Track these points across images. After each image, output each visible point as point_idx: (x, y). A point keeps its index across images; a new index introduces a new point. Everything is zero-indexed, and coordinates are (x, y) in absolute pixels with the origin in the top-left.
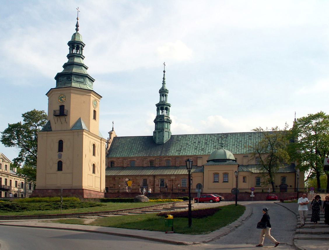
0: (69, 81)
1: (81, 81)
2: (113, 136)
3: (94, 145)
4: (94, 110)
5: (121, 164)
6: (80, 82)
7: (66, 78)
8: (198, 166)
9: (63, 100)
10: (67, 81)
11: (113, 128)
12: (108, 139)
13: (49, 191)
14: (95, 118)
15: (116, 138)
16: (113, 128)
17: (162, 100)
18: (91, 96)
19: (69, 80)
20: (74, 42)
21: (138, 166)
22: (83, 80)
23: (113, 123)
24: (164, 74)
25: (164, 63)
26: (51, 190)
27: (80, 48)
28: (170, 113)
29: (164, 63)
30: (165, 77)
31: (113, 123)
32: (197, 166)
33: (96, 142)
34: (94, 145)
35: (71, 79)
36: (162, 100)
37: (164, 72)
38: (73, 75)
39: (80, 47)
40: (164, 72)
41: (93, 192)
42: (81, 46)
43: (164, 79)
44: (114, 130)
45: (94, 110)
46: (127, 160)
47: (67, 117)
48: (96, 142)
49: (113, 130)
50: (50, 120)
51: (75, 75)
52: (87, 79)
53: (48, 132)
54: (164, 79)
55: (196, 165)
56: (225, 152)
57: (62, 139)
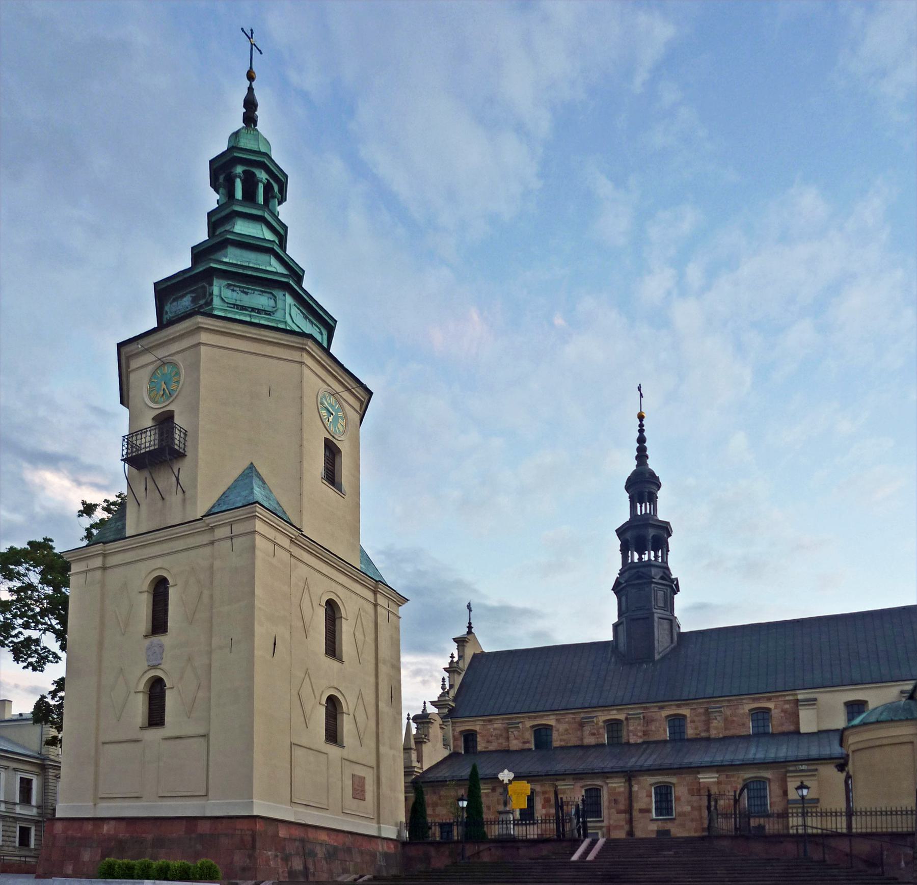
1: (260, 307)
2: (469, 652)
3: (332, 608)
4: (326, 439)
5: (500, 741)
6: (253, 310)
8: (802, 731)
11: (470, 623)
12: (452, 657)
13: (106, 828)
14: (331, 476)
15: (480, 658)
16: (470, 623)
17: (639, 513)
18: (302, 363)
21: (563, 744)
22: (272, 303)
23: (470, 611)
24: (641, 426)
25: (640, 385)
26: (112, 823)
28: (669, 556)
29: (640, 385)
30: (645, 434)
31: (470, 611)
32: (797, 732)
33: (341, 591)
34: (332, 608)
36: (639, 513)
37: (641, 417)
38: (219, 277)
40: (641, 417)
41: (323, 837)
43: (641, 440)
44: (473, 630)
45: (326, 439)
46: (520, 725)
47: (184, 467)
48: (341, 591)
49: (470, 632)
51: (229, 279)
52: (289, 299)
54: (641, 440)
55: (792, 728)
57: (165, 574)
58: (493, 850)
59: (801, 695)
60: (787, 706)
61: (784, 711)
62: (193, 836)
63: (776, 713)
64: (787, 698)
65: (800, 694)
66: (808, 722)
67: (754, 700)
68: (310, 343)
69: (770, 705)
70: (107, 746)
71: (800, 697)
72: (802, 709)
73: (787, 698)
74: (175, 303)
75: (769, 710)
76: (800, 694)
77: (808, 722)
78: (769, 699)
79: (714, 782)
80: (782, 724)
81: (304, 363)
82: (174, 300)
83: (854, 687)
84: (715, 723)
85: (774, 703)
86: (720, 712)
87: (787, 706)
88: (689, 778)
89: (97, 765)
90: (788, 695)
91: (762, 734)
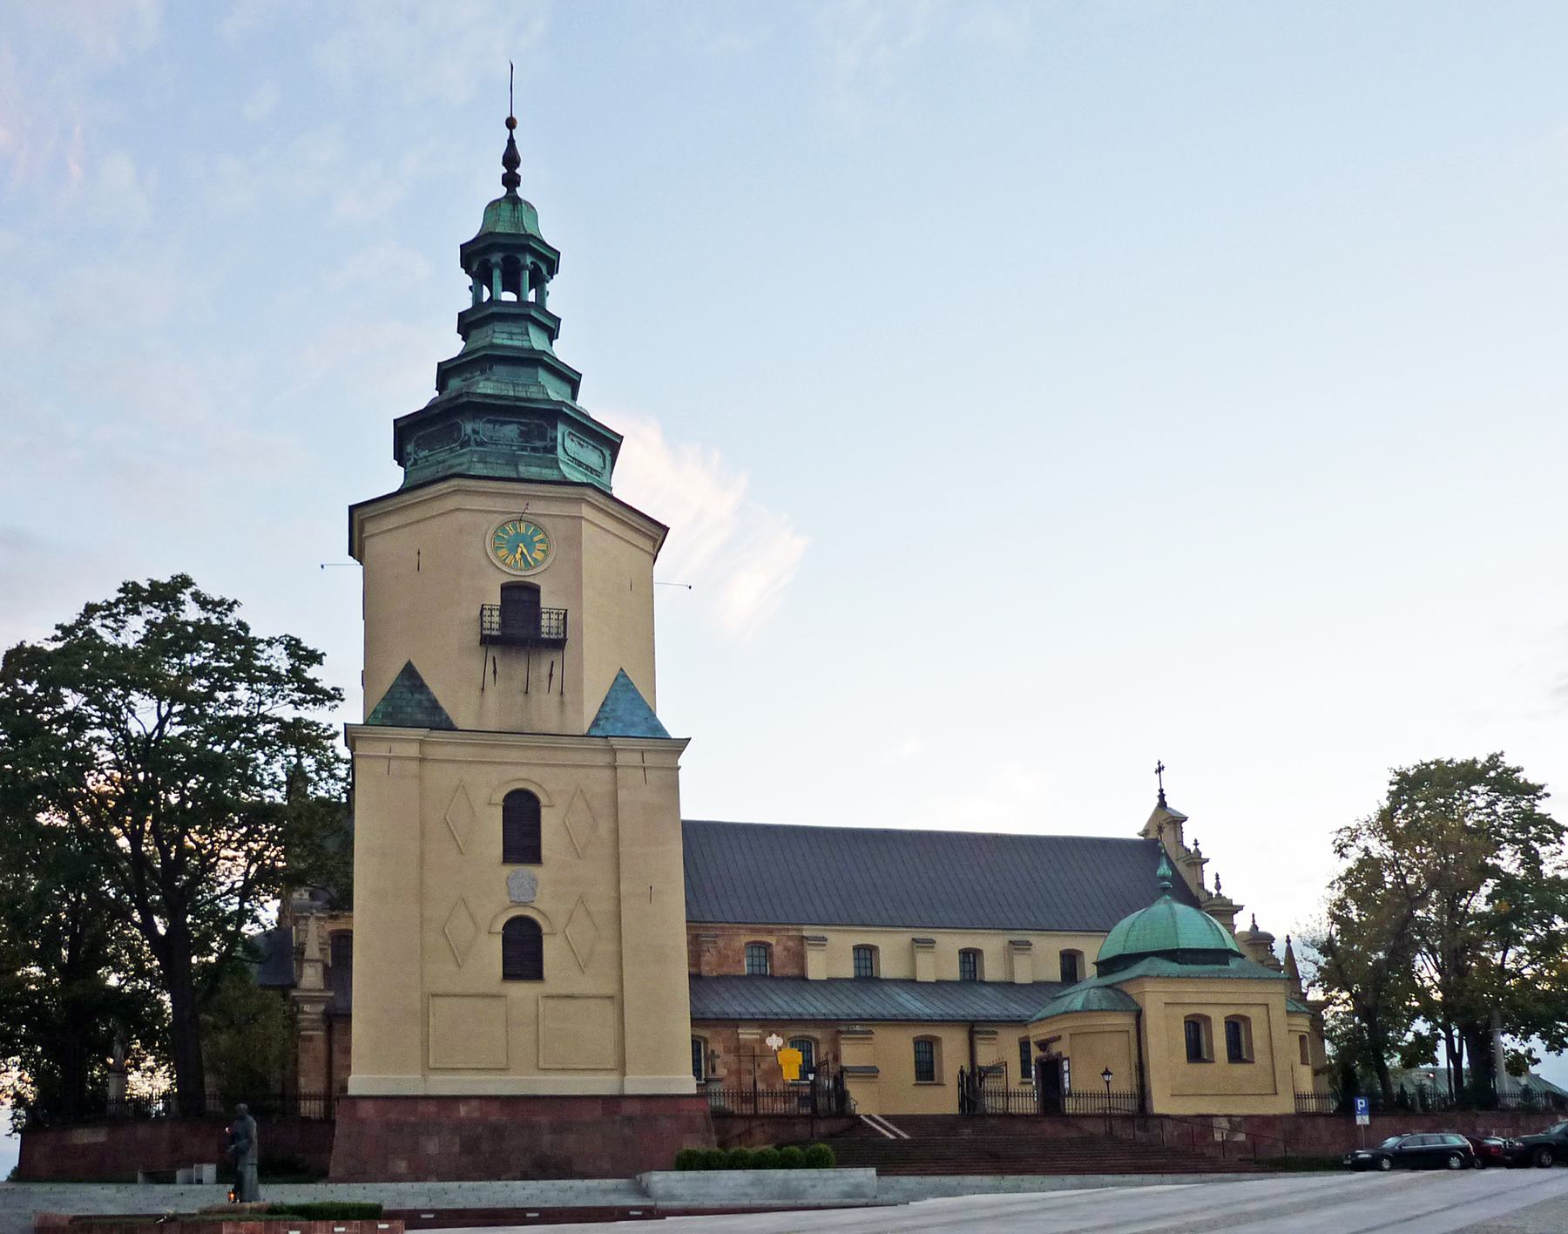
0: (534, 449)
7: (514, 427)
9: (518, 556)
10: (524, 449)
19: (538, 444)
20: (524, 242)
27: (526, 274)
35: (549, 443)
39: (526, 267)
42: (529, 260)
50: (415, 663)
53: (436, 733)
56: (1173, 914)
58: (766, 1127)
59: (808, 931)
60: (791, 944)
61: (787, 949)
62: (618, 1118)
63: (778, 950)
64: (790, 933)
65: (808, 929)
66: (817, 968)
67: (754, 931)
68: (589, 492)
69: (772, 940)
70: (437, 1000)
71: (805, 934)
72: (810, 950)
73: (790, 933)
74: (490, 426)
75: (770, 945)
76: (808, 929)
77: (817, 968)
78: (770, 932)
79: (756, 1039)
80: (784, 966)
81: (582, 518)
82: (489, 421)
83: (866, 929)
84: (707, 957)
85: (775, 938)
86: (715, 942)
87: (791, 944)
88: (726, 1032)
89: (426, 1023)
90: (792, 929)
91: (762, 978)
